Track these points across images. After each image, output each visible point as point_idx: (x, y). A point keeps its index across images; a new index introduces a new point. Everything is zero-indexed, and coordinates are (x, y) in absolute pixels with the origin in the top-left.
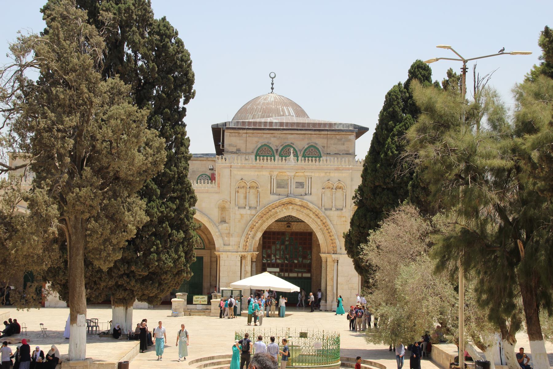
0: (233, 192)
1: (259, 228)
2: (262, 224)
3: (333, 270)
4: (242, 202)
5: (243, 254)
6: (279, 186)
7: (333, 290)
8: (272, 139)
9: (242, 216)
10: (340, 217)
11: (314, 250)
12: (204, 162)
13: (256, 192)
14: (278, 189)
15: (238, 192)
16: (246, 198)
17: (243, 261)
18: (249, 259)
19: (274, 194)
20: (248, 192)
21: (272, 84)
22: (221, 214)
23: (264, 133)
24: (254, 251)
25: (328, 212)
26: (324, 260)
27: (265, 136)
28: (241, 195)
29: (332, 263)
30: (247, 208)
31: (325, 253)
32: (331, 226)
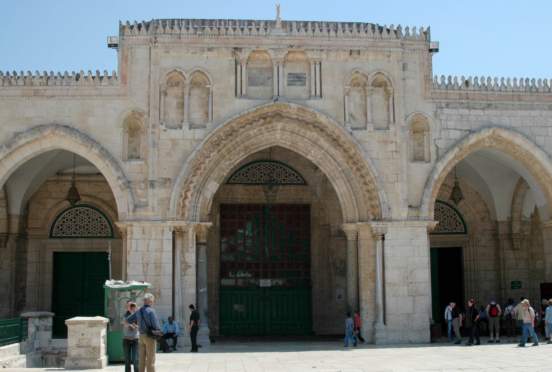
1: (212, 170)
2: (217, 163)
3: (375, 256)
4: (173, 115)
5: (177, 224)
6: (252, 82)
7: (375, 297)
9: (173, 140)
10: (385, 142)
11: (316, 236)
13: (204, 95)
14: (253, 88)
15: (166, 94)
16: (181, 106)
17: (179, 242)
18: (191, 236)
19: (242, 96)
20: (186, 92)
22: (130, 142)
24: (201, 221)
25: (358, 134)
26: (351, 237)
28: (172, 101)
29: (371, 242)
30: (186, 127)
31: (352, 222)
32: (367, 162)
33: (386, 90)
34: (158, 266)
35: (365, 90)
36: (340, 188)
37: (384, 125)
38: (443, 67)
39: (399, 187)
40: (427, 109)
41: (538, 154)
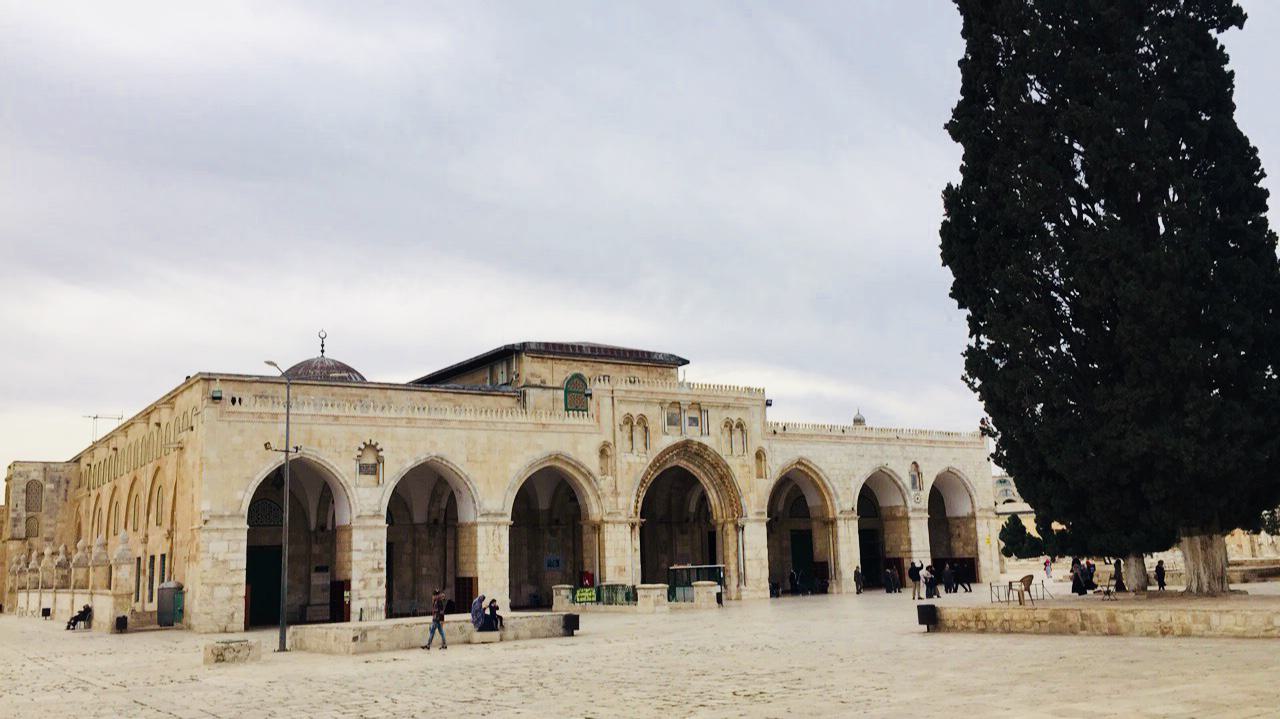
0: (618, 429)
3: (738, 541)
4: (627, 444)
8: (585, 368)
9: (629, 464)
10: (743, 466)
12: (498, 398)
18: (637, 528)
19: (667, 434)
21: (323, 346)
23: (574, 360)
26: (719, 528)
27: (575, 364)
29: (734, 533)
33: (742, 430)
34: (624, 551)
35: (731, 430)
36: (712, 496)
37: (741, 453)
38: (773, 415)
39: (751, 495)
40: (765, 445)
41: (821, 474)
